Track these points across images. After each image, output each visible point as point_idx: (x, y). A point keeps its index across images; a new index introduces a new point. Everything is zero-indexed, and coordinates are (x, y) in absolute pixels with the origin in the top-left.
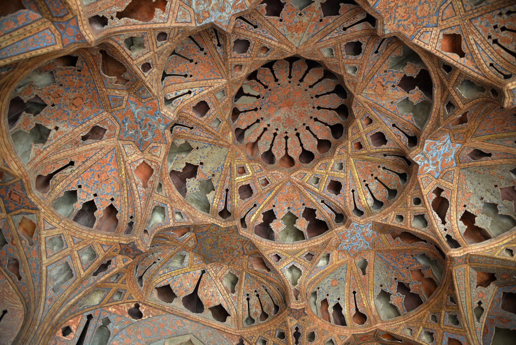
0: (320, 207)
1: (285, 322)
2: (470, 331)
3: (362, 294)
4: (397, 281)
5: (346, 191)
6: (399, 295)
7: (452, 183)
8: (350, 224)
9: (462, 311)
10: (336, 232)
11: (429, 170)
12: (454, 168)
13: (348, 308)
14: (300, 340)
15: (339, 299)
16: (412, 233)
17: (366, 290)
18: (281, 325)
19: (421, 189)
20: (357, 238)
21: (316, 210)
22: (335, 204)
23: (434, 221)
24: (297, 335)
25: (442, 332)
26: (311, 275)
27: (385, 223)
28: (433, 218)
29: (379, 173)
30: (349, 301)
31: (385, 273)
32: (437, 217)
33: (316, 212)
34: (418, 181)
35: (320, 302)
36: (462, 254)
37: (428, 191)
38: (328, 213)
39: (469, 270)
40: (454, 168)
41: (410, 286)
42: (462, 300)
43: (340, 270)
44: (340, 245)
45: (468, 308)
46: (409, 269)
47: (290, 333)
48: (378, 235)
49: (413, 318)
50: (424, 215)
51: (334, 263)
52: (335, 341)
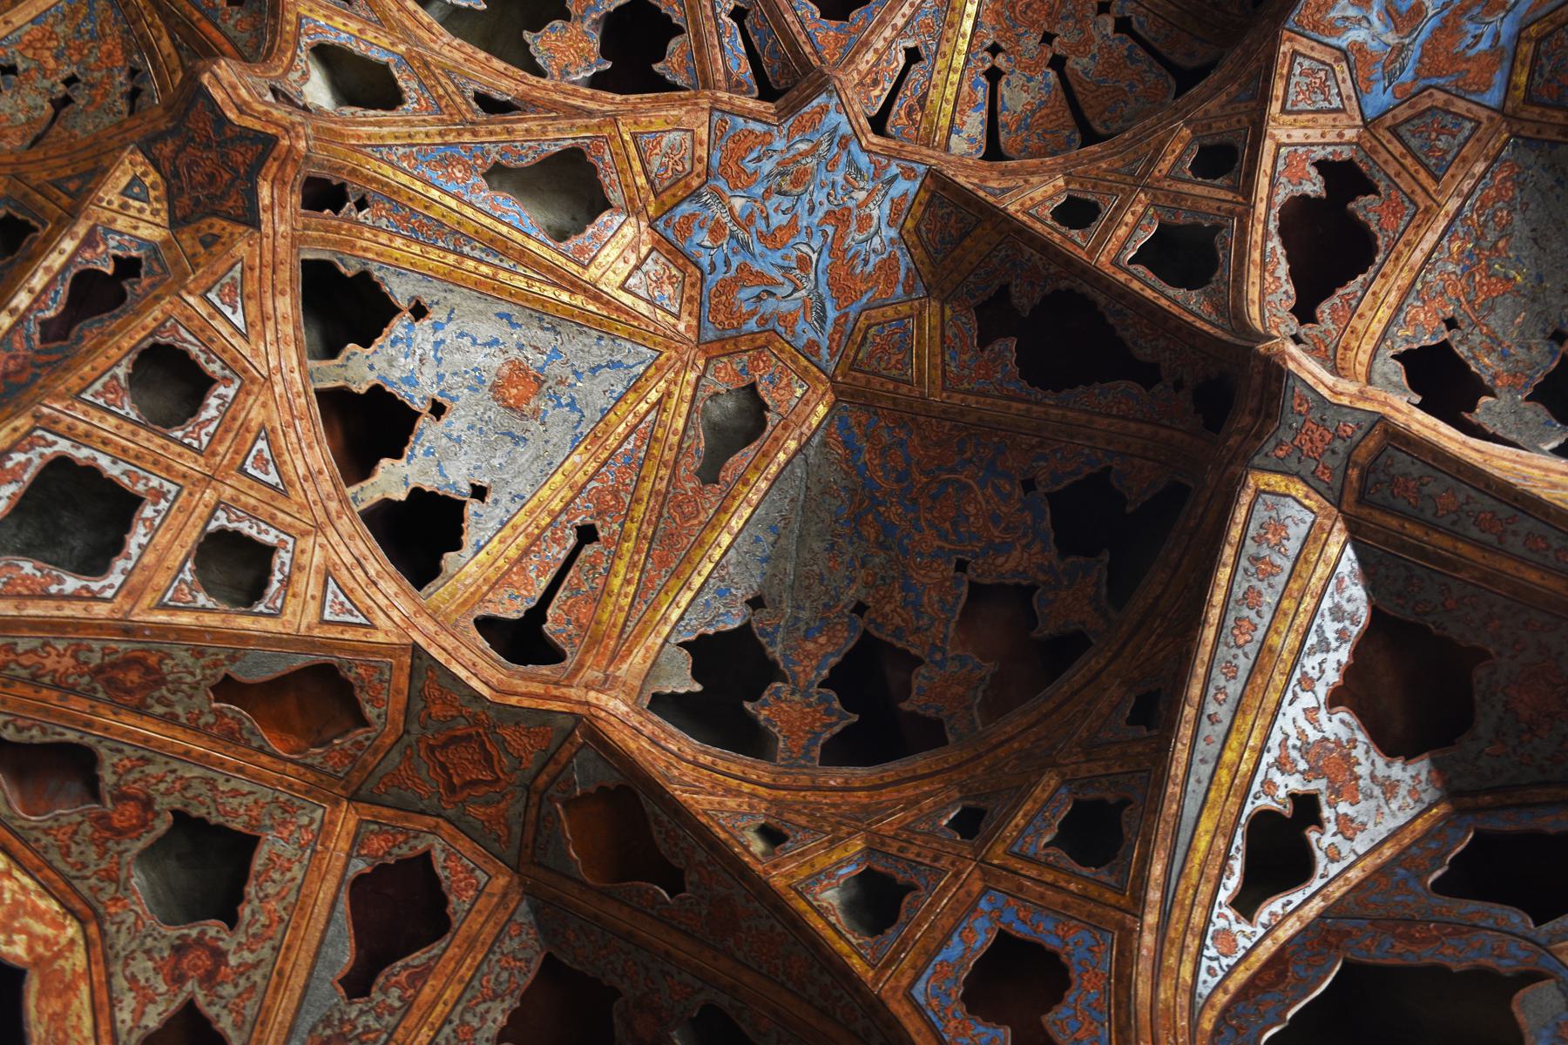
0: (709, 26)
1: (96, 173)
2: (1165, 915)
3: (621, 567)
4: (861, 623)
5: (882, 22)
6: (822, 700)
7: (1437, 179)
8: (808, 99)
9: (1177, 770)
10: (717, 100)
11: (1358, 35)
12: (1483, 114)
13: (492, 574)
14: (90, 330)
15: (479, 492)
16: (1101, 299)
17: (663, 562)
18: (56, 184)
19: (1265, 98)
20: (793, 225)
21: (679, 31)
22: (793, 44)
23: (1254, 273)
24: (97, 295)
25: (977, 886)
26: (436, 175)
27: (991, 199)
28: (1256, 255)
29: (1091, 39)
30: (526, 552)
31: (817, 545)
32: (1283, 269)
33: (673, 44)
34: (1271, 60)
35: (372, 378)
36: (1345, 401)
37: (1298, 135)
38: (728, 73)
39: (1333, 550)
40: (1483, 114)
41: (920, 678)
42: (1211, 708)
43: (600, 352)
44: (686, 208)
45: (1224, 775)
46: (971, 574)
47: (69, 245)
48: (909, 288)
49: (836, 798)
50: (1216, 228)
51: (592, 273)
52: (287, 582)
